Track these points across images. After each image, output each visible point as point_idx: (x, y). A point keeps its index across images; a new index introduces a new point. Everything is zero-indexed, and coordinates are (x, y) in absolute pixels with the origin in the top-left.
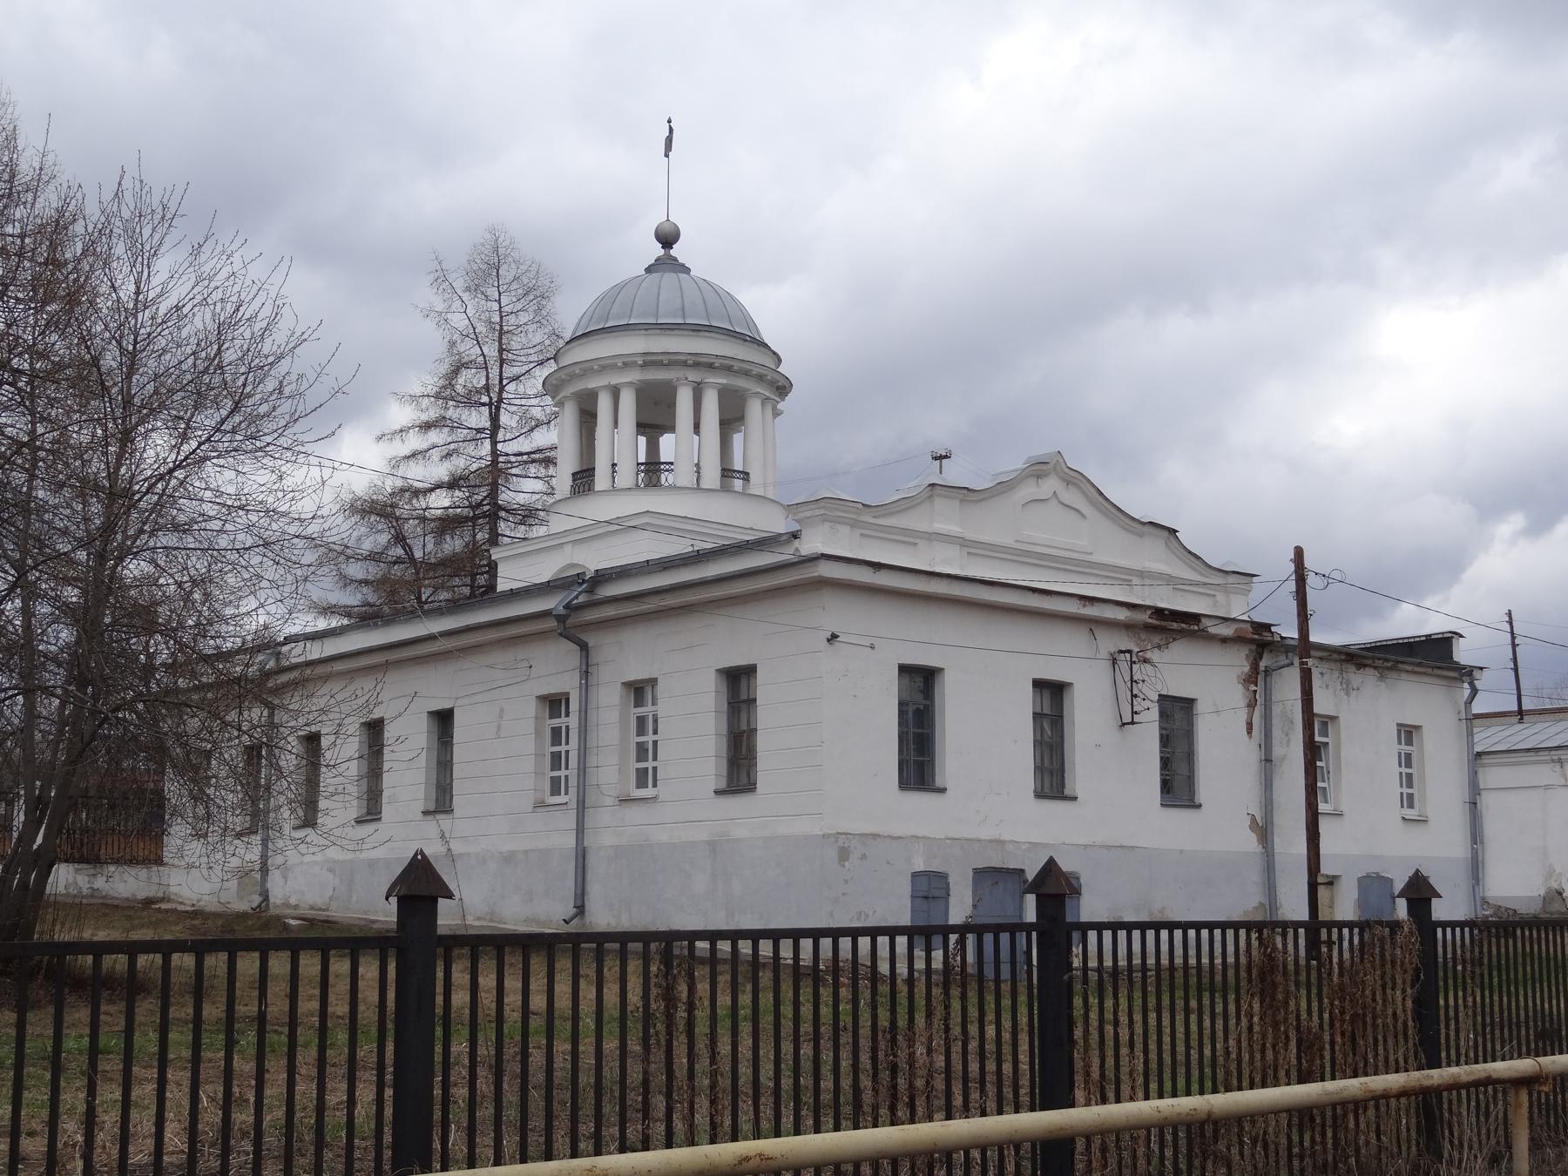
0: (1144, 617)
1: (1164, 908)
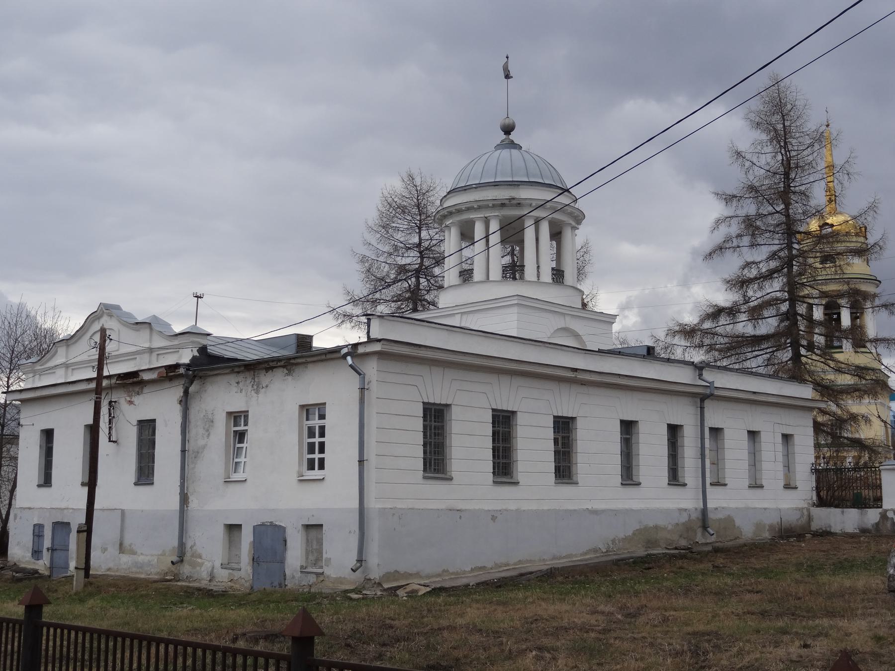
0: (113, 381)
1: (131, 544)
